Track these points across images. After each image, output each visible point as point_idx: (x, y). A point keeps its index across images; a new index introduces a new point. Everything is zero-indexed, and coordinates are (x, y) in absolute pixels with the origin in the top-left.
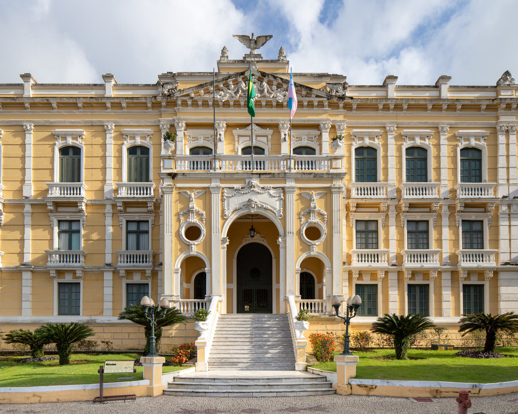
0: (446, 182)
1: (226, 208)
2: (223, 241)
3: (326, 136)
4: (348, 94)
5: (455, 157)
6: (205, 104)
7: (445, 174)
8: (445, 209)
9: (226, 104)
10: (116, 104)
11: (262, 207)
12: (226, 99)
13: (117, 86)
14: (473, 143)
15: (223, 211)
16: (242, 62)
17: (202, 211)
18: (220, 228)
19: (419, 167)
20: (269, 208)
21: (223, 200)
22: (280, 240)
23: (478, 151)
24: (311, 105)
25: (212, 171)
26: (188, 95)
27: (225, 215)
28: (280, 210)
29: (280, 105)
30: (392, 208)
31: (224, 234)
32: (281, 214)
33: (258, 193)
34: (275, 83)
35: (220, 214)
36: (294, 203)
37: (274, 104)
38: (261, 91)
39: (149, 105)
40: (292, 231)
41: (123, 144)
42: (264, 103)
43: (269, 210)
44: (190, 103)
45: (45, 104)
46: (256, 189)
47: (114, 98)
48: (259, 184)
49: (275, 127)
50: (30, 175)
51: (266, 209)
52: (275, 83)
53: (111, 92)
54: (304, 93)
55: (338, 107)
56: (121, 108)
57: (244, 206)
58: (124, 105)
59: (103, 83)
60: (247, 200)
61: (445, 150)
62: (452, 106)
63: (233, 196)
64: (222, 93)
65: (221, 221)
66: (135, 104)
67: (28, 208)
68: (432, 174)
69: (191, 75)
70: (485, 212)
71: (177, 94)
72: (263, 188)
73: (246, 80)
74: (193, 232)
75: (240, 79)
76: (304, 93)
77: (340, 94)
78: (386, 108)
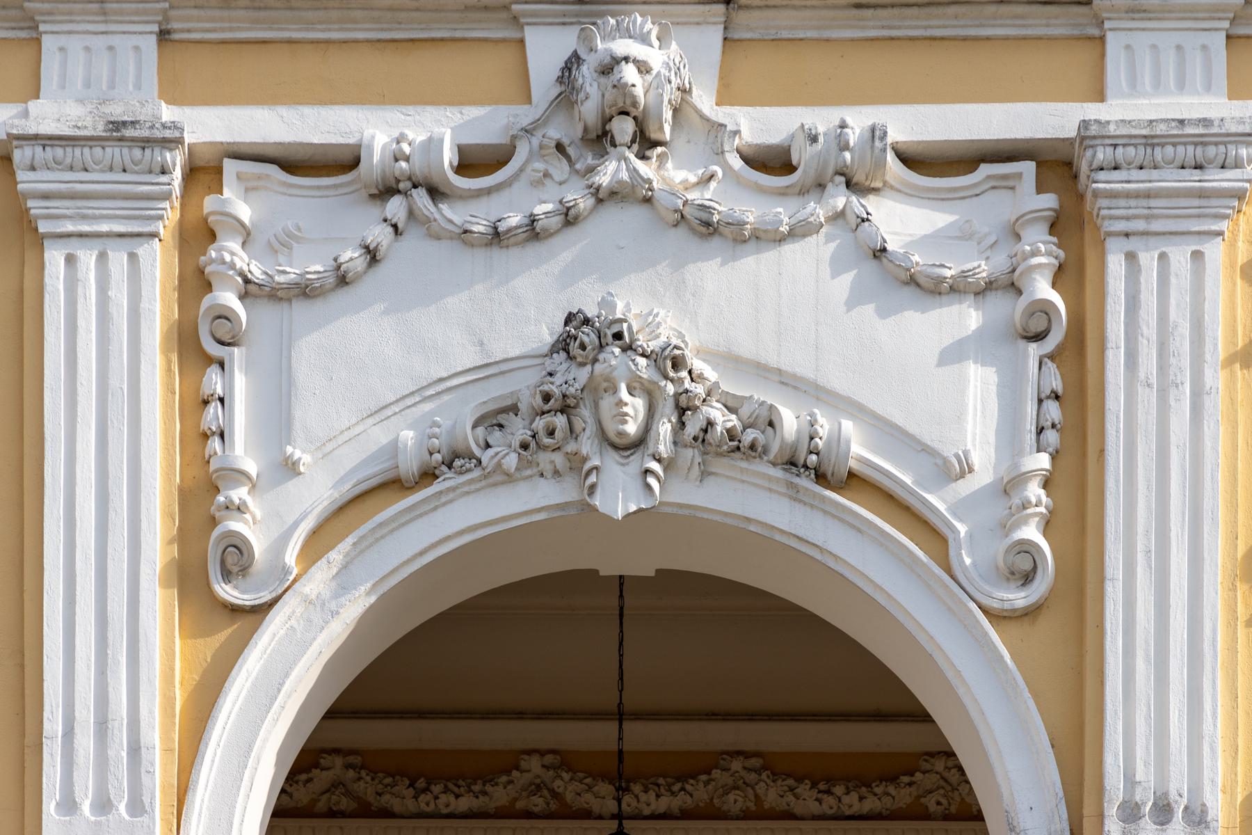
1: (243, 453)
15: (202, 495)
18: (154, 736)
20: (859, 449)
27: (236, 558)
28: (1010, 485)
32: (1031, 532)
33: (706, 227)
35: (157, 549)
36: (1215, 378)
40: (1178, 786)
43: (854, 482)
46: (671, 174)
48: (704, 100)
51: (815, 469)
57: (493, 419)
60: (546, 332)
63: (343, 280)
72: (772, 162)
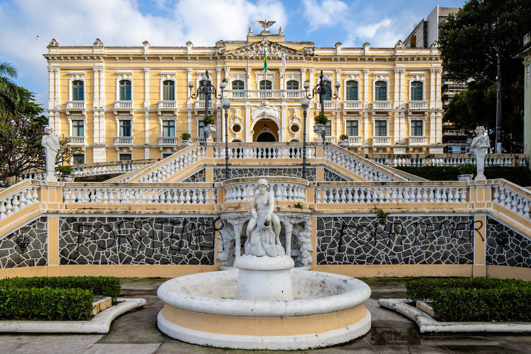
0: (367, 100)
2: (252, 132)
3: (304, 77)
4: (316, 52)
5: (372, 86)
6: (241, 58)
7: (367, 95)
8: (366, 115)
9: (252, 58)
10: (194, 58)
11: (270, 116)
12: (251, 56)
13: (193, 48)
14: (382, 78)
15: (251, 117)
16: (260, 36)
17: (241, 118)
19: (353, 91)
21: (251, 112)
22: (279, 131)
23: (385, 83)
24: (296, 58)
25: (246, 98)
26: (231, 54)
29: (280, 59)
30: (339, 114)
31: (252, 129)
34: (277, 47)
37: (277, 58)
38: (270, 52)
39: (211, 58)
41: (197, 79)
42: (271, 58)
44: (232, 58)
45: (156, 58)
46: (267, 107)
47: (192, 55)
49: (277, 70)
50: (148, 96)
51: (272, 116)
52: (277, 47)
53: (190, 51)
54: (292, 52)
55: (310, 60)
56: (196, 59)
58: (197, 58)
59: (186, 46)
61: (367, 83)
62: (371, 59)
64: (249, 52)
65: (250, 122)
66: (203, 58)
67: (147, 114)
68: (360, 96)
69: (233, 42)
70: (388, 116)
71: (226, 53)
73: (262, 45)
74: (237, 128)
75: (259, 45)
76: (292, 52)
77: (311, 53)
78: (336, 60)
